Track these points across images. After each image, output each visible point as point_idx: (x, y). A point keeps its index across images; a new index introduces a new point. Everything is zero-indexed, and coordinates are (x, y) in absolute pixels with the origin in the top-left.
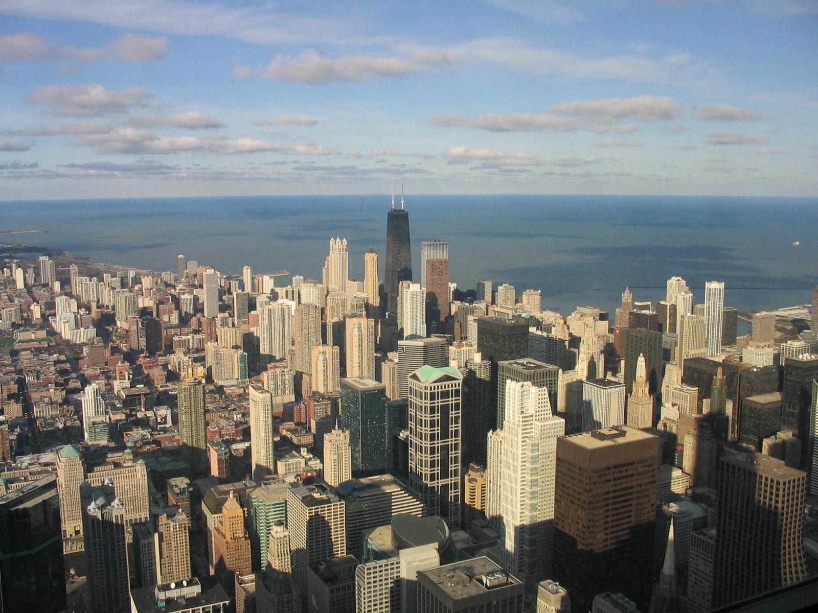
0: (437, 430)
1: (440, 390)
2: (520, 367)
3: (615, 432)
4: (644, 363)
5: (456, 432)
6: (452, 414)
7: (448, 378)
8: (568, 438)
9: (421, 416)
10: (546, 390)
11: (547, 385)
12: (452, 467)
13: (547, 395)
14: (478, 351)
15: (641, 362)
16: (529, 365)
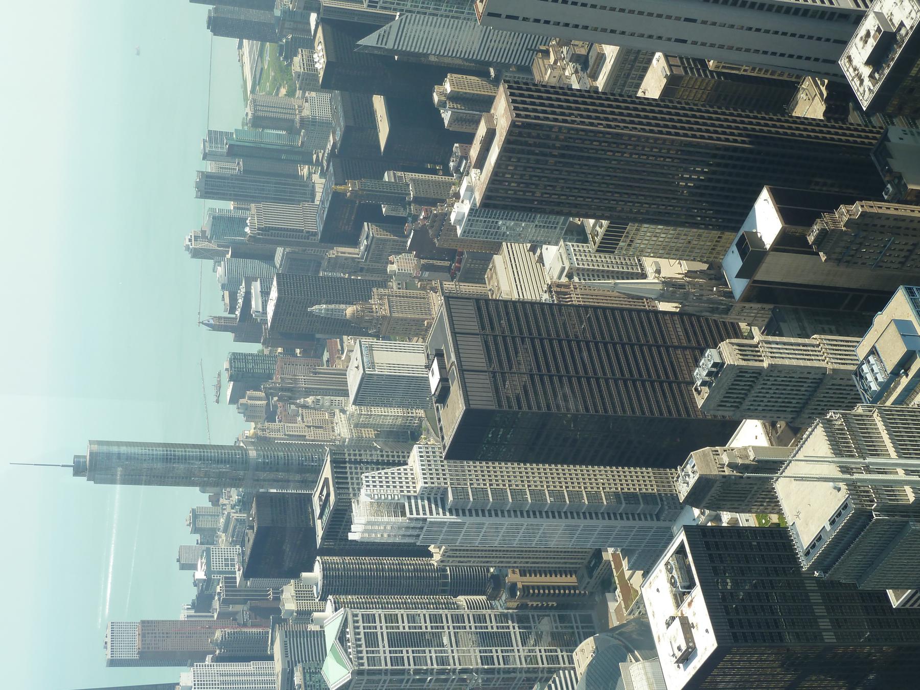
0: (431, 653)
1: (364, 648)
2: (327, 511)
3: (435, 365)
4: (324, 306)
5: (435, 619)
6: (404, 627)
7: (342, 638)
8: (448, 441)
9: (407, 682)
10: (367, 474)
11: (357, 473)
12: (493, 626)
13: (376, 473)
14: (296, 576)
15: (320, 309)
16: (323, 498)
